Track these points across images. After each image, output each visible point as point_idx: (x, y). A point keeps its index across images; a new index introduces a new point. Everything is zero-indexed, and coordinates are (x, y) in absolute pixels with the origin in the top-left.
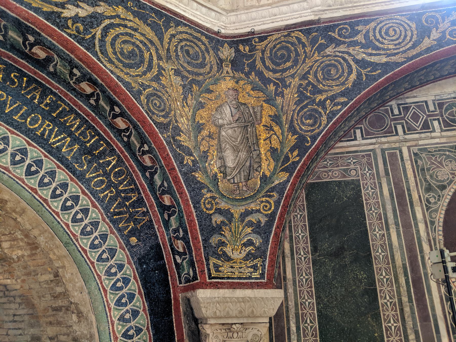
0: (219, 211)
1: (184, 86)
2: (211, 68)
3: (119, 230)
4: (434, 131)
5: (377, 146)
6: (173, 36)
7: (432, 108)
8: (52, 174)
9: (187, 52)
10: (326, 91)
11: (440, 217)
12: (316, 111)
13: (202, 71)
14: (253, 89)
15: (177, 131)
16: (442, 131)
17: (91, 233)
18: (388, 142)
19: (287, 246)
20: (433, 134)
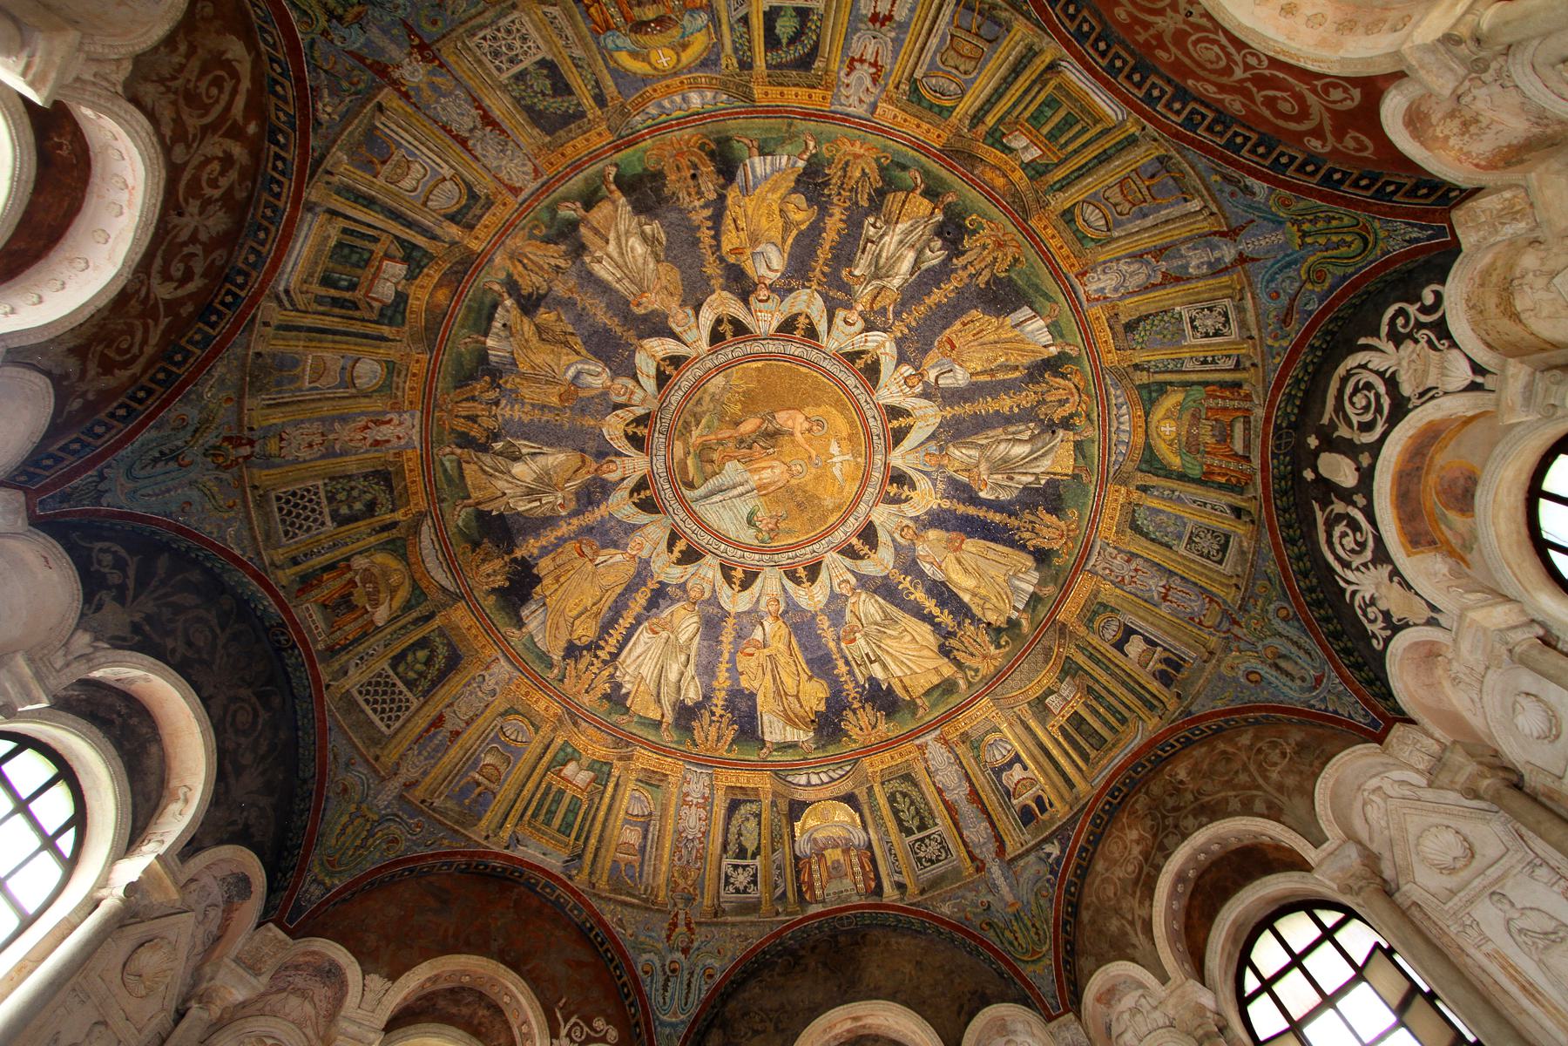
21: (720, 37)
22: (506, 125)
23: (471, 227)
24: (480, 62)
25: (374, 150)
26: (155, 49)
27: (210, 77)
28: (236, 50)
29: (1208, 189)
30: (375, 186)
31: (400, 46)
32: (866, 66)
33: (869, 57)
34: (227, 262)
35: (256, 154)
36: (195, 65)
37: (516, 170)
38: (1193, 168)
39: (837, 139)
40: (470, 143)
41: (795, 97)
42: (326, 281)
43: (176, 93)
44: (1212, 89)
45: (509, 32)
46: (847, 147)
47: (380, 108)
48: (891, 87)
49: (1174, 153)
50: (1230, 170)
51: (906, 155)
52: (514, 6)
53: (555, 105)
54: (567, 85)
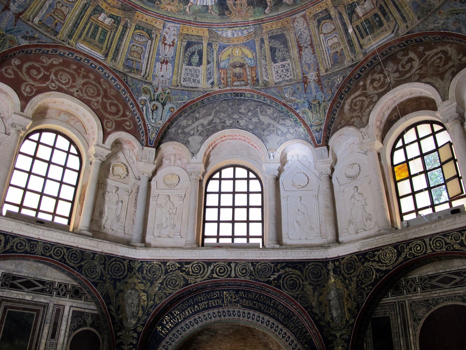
0: (332, 335)
1: (313, 289)
2: (324, 276)
3: (300, 342)
4: (418, 293)
5: (396, 300)
6: (307, 269)
7: (417, 281)
8: (277, 327)
9: (313, 273)
10: (366, 283)
11: (418, 333)
12: (362, 292)
13: (320, 279)
14: (341, 282)
15: (312, 308)
16: (421, 292)
17: (292, 344)
18: (400, 298)
19: (365, 345)
20: (418, 294)
21: (217, 56)
22: (296, 44)
23: (326, 10)
24: (293, 70)
25: (337, 58)
26: (355, 126)
27: (355, 108)
28: (347, 107)
29: (36, 29)
30: (344, 46)
31: (310, 86)
32: (168, 43)
33: (167, 47)
34: (400, 51)
35: (367, 75)
36: (354, 114)
37: (300, 25)
38: (46, 35)
39: (178, 12)
40: (309, 43)
41: (194, 31)
42: (381, 24)
43: (362, 113)
44: (55, 63)
45: (281, 76)
46: (173, 8)
47: (326, 71)
48: (159, 35)
49: (55, 38)
50: (35, 42)
51: (149, 7)
52: (276, 84)
53: (277, 44)
54: (271, 51)
